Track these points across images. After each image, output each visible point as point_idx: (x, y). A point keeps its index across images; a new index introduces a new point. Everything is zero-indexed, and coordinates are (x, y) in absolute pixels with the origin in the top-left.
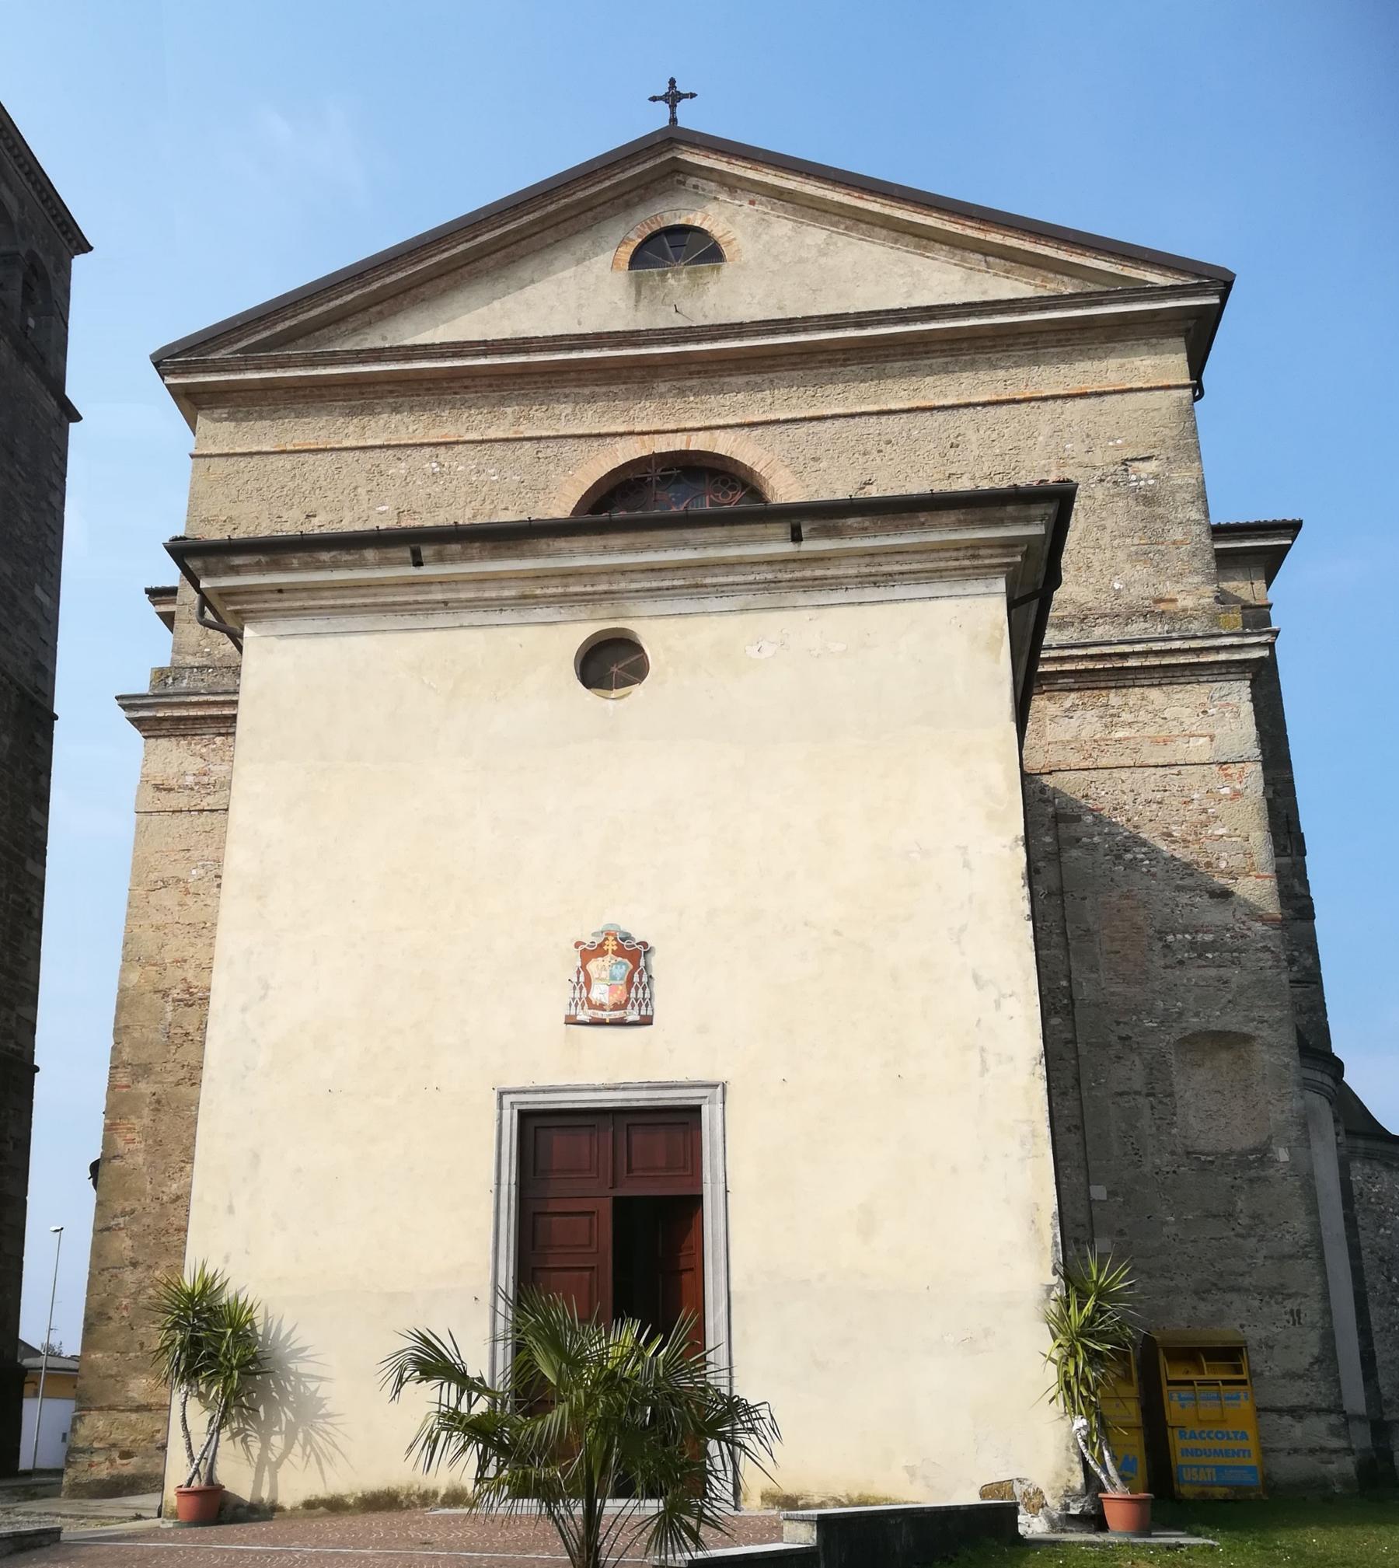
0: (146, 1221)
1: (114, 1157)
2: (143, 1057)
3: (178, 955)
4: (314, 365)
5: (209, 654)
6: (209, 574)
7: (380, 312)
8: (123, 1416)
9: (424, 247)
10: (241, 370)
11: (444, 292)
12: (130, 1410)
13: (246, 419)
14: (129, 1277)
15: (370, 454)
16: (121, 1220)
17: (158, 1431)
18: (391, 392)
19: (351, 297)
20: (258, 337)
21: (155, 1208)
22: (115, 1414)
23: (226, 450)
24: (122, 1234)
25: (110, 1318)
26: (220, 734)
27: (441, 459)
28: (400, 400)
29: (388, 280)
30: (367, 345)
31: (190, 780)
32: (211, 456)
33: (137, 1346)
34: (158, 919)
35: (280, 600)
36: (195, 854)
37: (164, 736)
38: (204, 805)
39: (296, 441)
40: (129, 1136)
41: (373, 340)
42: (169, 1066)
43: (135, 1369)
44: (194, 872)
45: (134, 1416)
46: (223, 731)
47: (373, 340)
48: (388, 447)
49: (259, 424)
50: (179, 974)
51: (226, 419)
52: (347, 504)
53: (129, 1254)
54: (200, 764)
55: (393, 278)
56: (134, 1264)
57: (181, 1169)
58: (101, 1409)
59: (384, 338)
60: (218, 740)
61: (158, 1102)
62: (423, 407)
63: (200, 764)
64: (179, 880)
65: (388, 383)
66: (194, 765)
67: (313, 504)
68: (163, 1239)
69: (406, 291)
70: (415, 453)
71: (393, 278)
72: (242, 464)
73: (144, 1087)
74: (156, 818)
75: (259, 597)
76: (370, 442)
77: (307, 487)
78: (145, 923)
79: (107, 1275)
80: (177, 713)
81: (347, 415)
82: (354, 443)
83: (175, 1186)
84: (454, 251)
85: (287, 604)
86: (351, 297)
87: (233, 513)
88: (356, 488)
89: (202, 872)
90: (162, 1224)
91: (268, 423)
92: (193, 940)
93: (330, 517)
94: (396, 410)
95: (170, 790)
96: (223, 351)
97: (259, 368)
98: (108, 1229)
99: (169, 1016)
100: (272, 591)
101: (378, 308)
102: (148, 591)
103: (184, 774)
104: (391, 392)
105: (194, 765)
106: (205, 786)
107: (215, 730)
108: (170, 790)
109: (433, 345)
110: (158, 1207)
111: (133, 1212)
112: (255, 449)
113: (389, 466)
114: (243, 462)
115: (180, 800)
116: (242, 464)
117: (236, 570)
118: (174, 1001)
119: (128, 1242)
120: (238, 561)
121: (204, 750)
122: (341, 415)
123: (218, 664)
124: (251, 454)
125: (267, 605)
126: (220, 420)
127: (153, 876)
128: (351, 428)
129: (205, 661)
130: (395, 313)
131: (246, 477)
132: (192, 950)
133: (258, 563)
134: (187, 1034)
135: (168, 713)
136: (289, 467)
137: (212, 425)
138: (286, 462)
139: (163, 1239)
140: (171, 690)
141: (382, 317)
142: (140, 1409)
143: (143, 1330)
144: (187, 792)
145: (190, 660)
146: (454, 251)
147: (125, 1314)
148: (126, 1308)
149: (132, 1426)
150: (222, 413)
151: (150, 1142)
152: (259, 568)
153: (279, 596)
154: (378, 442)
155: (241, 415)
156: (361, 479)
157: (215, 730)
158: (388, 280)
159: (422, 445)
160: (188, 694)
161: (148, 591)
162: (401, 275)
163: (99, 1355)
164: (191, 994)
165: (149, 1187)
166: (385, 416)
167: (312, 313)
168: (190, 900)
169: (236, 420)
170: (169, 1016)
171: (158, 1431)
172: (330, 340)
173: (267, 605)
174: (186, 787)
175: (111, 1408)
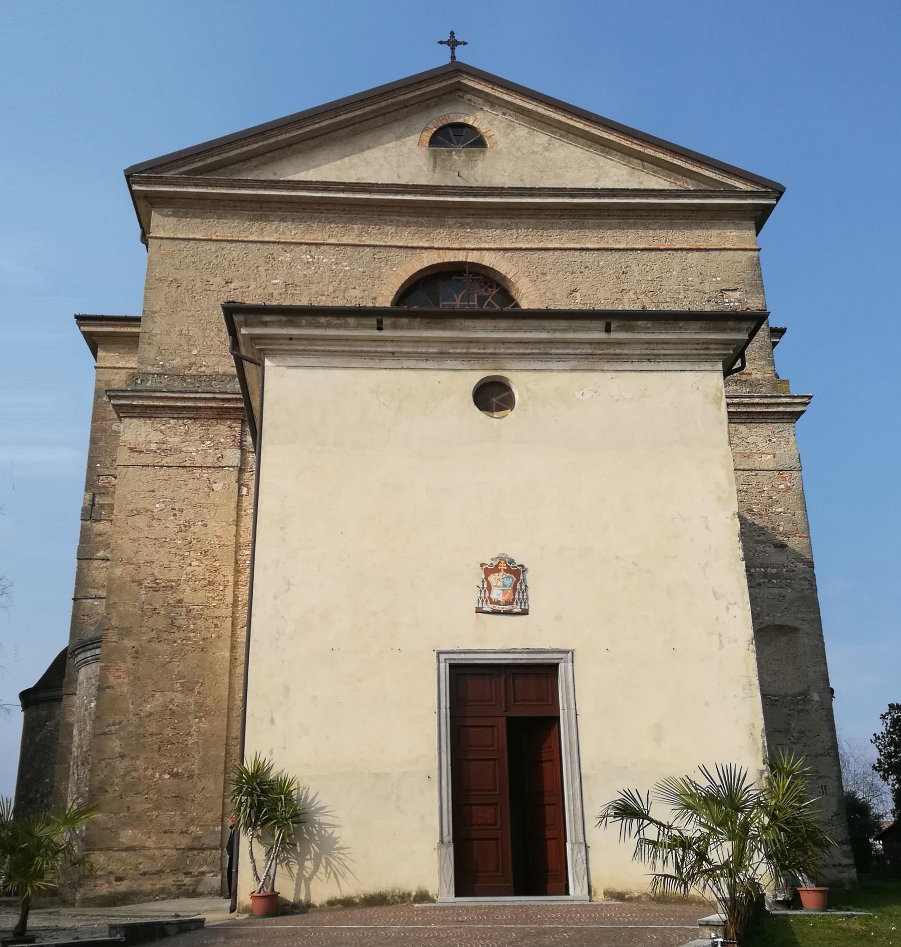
0: (131, 729)
1: (107, 687)
2: (127, 624)
3: (148, 558)
4: (232, 186)
5: (163, 366)
6: (247, 324)
7: (272, 157)
8: (117, 854)
9: (304, 120)
10: (184, 186)
11: (312, 149)
12: (122, 850)
13: (185, 216)
14: (122, 766)
15: (266, 246)
16: (113, 728)
17: (140, 863)
18: (280, 208)
19: (257, 145)
20: (195, 166)
21: (135, 720)
22: (111, 853)
23: (172, 236)
24: (114, 737)
25: (106, 791)
26: (174, 418)
27: (313, 254)
28: (286, 214)
29: (280, 138)
30: (263, 178)
31: (153, 446)
32: (162, 238)
33: (125, 809)
34: (133, 534)
35: (290, 344)
36: (158, 494)
37: (136, 417)
38: (163, 462)
39: (218, 234)
40: (117, 674)
41: (267, 174)
42: (143, 629)
43: (124, 824)
44: (157, 505)
45: (124, 854)
46: (175, 416)
47: (267, 174)
48: (279, 243)
49: (194, 220)
50: (149, 571)
51: (171, 216)
52: (252, 276)
53: (118, 749)
54: (160, 436)
55: (284, 137)
56: (122, 756)
57: (153, 696)
58: (101, 850)
59: (275, 174)
60: (172, 421)
61: (137, 652)
62: (301, 220)
63: (160, 436)
64: (147, 511)
65: (279, 202)
66: (156, 437)
67: (230, 275)
68: (141, 741)
69: (289, 145)
70: (296, 248)
71: (284, 137)
72: (183, 246)
73: (128, 643)
74: (131, 469)
75: (276, 341)
76: (267, 239)
77: (226, 263)
78: (125, 537)
79: (103, 764)
80: (146, 403)
81: (251, 220)
82: (257, 239)
83: (149, 706)
84: (322, 124)
85: (294, 347)
86: (257, 145)
87: (178, 276)
88: (258, 267)
89: (163, 505)
90: (141, 731)
91: (199, 220)
92: (158, 549)
93: (241, 284)
94: (283, 220)
95: (140, 452)
96: (172, 172)
97: (196, 185)
98: (104, 734)
99: (143, 598)
100: (285, 339)
101: (272, 154)
102: (77, 317)
103: (150, 442)
104: (280, 208)
105: (156, 437)
106: (164, 450)
107: (170, 415)
108: (140, 452)
109: (311, 182)
110: (137, 721)
111: (121, 723)
112: (191, 236)
113: (280, 255)
114: (183, 245)
115: (148, 459)
116: (183, 246)
117: (265, 324)
118: (146, 587)
119: (118, 743)
120: (267, 318)
121: (163, 428)
122: (247, 219)
123: (168, 372)
124: (189, 240)
125: (281, 347)
126: (167, 216)
127: (130, 507)
128: (254, 229)
129: (160, 370)
130: (281, 159)
131: (185, 253)
132: (157, 556)
133: (280, 321)
134: (155, 609)
135: (140, 402)
136: (214, 250)
137: (162, 219)
138: (212, 246)
139: (141, 741)
140: (139, 387)
141: (273, 160)
142: (127, 849)
143: (129, 799)
144: (152, 454)
145: (150, 369)
146: (322, 124)
147: (116, 788)
148: (117, 784)
149: (120, 860)
150: (169, 211)
151: (131, 678)
152: (281, 324)
153: (291, 342)
154: (272, 239)
155: (181, 214)
156: (261, 261)
157: (170, 415)
158: (280, 138)
159: (301, 244)
160: (155, 391)
161: (77, 317)
162: (289, 135)
163: (100, 815)
164: (157, 584)
165: (131, 707)
166: (276, 223)
167: (231, 154)
168: (155, 523)
169: (178, 217)
170: (143, 598)
171: (140, 863)
172: (239, 172)
173: (281, 347)
174: (151, 451)
175: (109, 849)
